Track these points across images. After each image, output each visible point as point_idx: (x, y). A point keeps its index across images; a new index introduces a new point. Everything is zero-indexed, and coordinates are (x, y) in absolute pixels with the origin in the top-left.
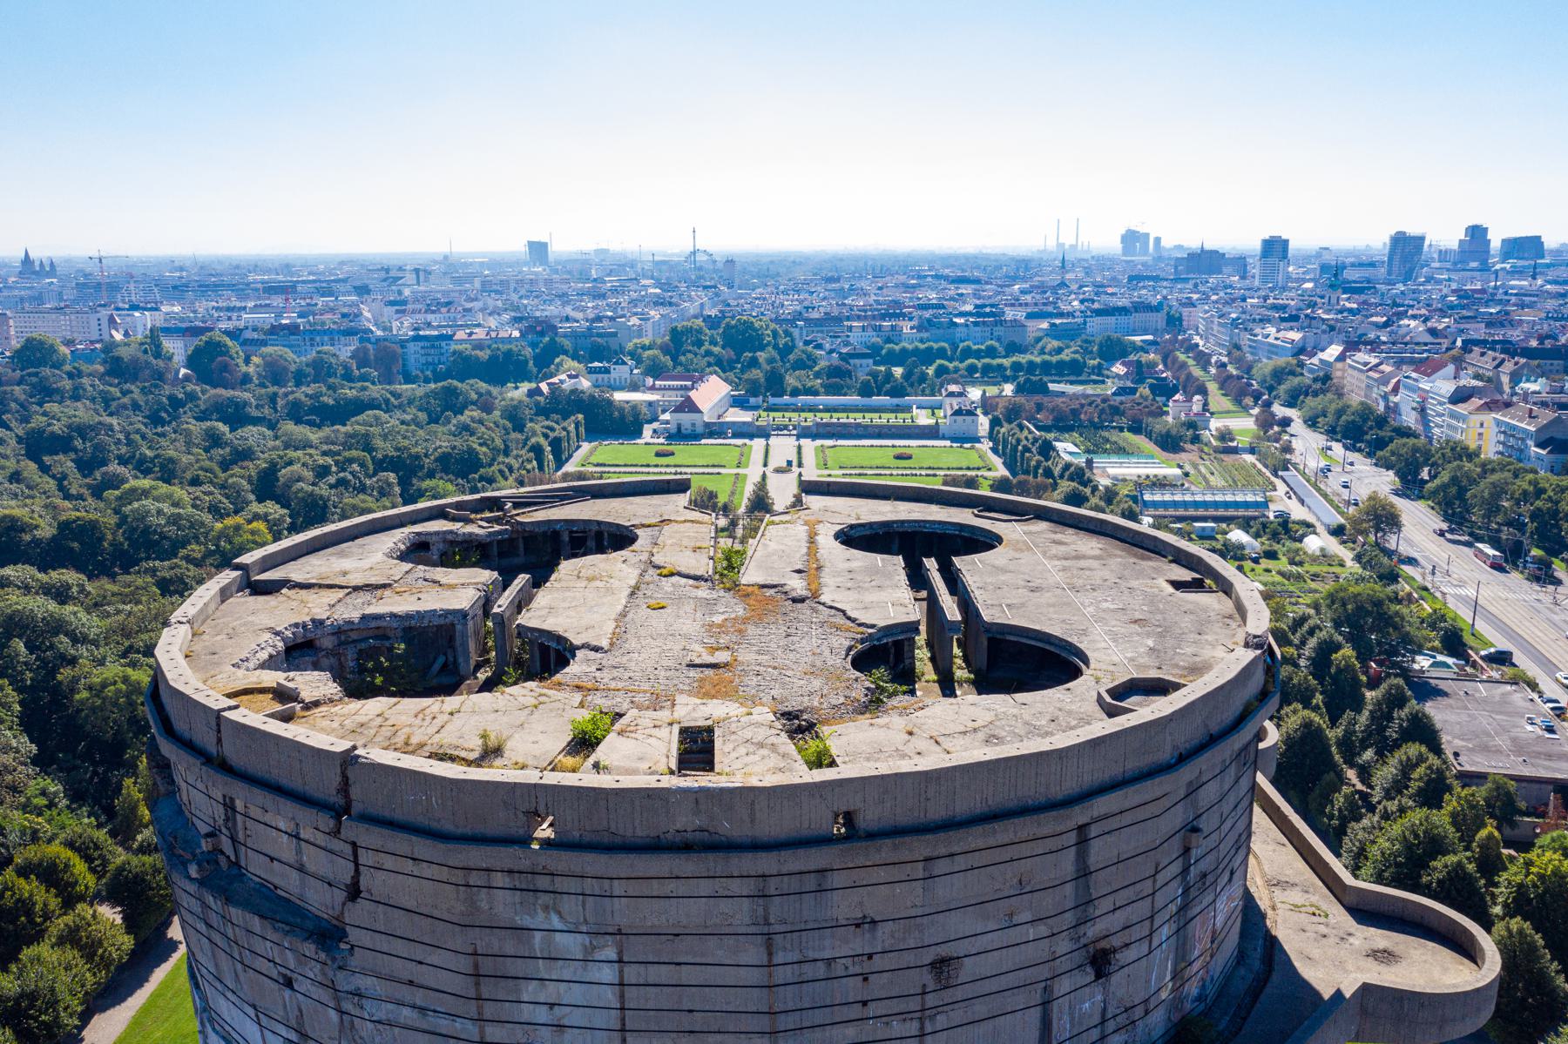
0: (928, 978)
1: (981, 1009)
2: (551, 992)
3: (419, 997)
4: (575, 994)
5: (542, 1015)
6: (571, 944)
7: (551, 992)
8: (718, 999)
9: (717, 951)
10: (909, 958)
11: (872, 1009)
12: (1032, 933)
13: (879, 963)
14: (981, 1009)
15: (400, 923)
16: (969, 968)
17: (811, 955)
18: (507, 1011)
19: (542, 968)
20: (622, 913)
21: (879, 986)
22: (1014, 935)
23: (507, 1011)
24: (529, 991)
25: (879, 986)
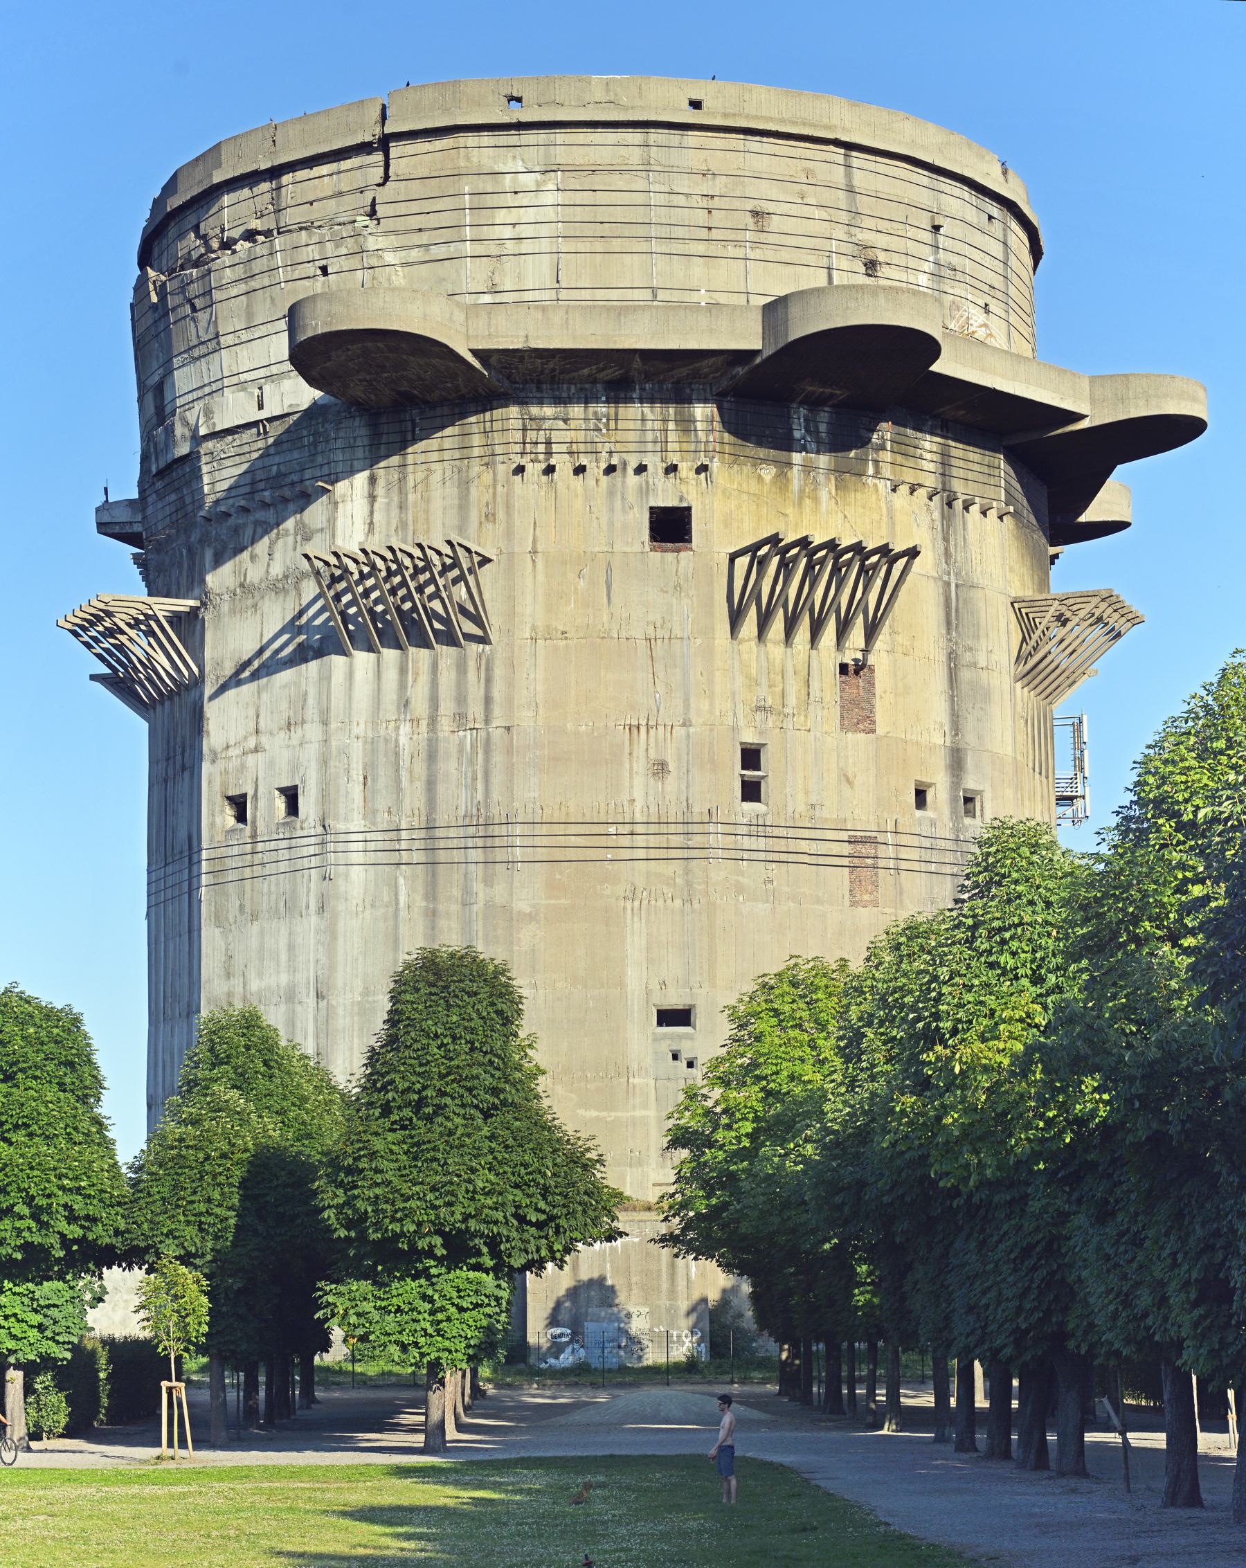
0: (749, 221)
1: (785, 255)
2: (512, 216)
3: (424, 238)
4: (530, 215)
5: (508, 232)
6: (528, 181)
7: (512, 216)
8: (619, 214)
9: (618, 181)
10: (737, 204)
11: (715, 234)
12: (817, 213)
13: (716, 203)
14: (785, 255)
15: (416, 189)
16: (775, 223)
17: (677, 190)
18: (487, 232)
19: (510, 200)
20: (561, 155)
21: (718, 219)
22: (807, 211)
23: (487, 232)
24: (501, 216)
25: (718, 219)
